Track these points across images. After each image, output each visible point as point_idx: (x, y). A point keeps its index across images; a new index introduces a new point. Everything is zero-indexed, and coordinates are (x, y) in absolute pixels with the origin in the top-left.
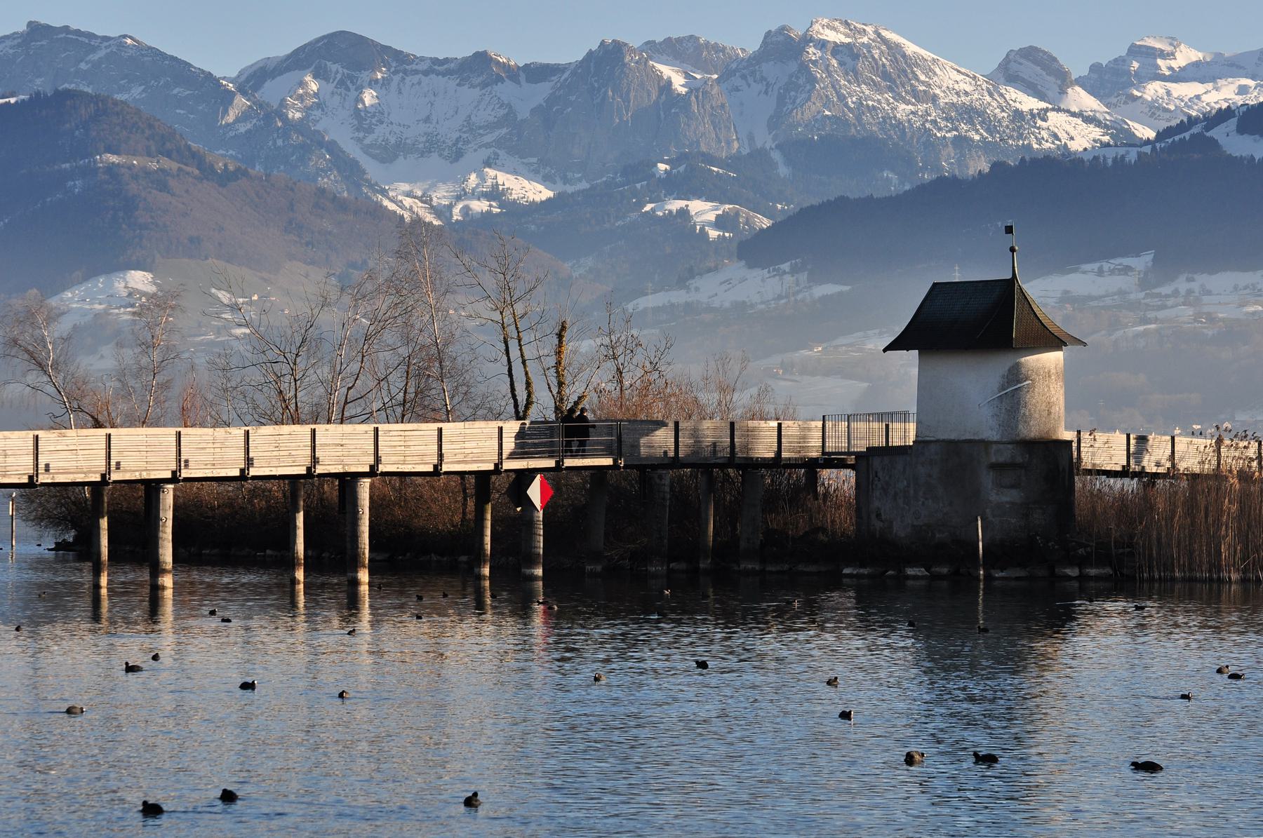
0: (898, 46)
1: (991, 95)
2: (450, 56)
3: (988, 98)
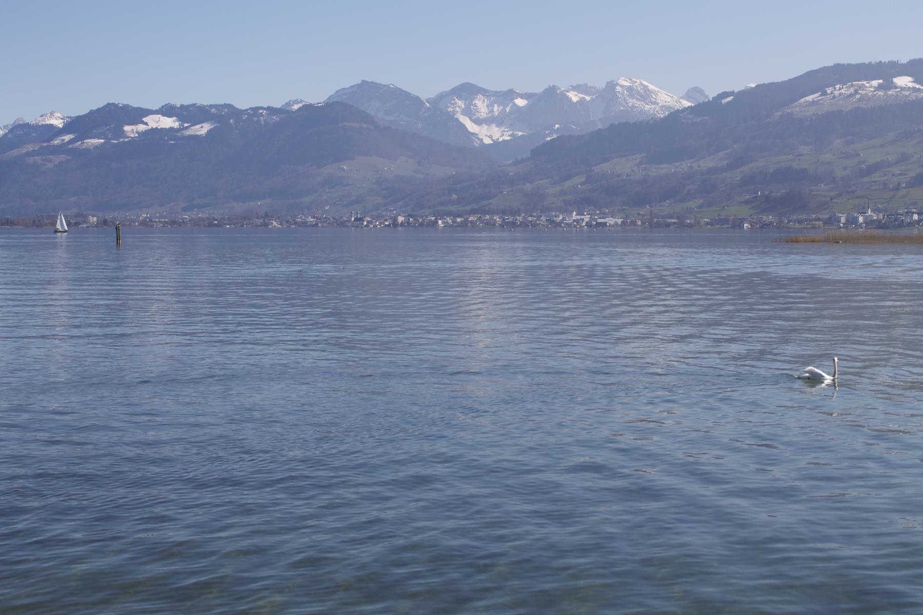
0: (647, 86)
1: (677, 102)
2: (501, 90)
3: (676, 103)
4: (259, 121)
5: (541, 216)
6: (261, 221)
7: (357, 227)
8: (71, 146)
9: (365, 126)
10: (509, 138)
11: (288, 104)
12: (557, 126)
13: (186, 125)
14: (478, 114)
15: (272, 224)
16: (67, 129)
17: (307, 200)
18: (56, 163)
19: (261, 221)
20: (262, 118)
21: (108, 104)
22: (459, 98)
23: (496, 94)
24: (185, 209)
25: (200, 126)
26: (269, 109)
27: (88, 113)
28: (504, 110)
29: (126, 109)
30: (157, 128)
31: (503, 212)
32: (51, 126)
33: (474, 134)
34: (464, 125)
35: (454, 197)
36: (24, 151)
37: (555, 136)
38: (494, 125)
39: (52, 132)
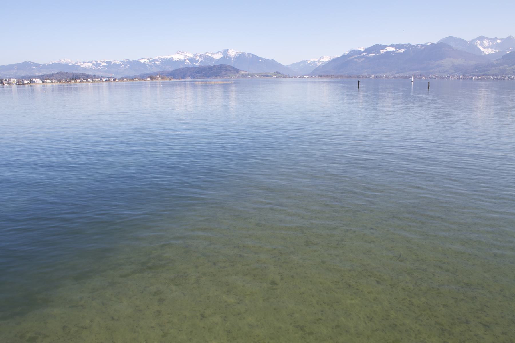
4: (418, 48)
5: (506, 77)
6: (419, 77)
7: (448, 79)
8: (366, 56)
9: (449, 49)
10: (494, 52)
11: (426, 43)
12: (511, 48)
13: (397, 50)
14: (484, 45)
15: (423, 78)
16: (365, 51)
17: (431, 71)
18: (362, 60)
19: (419, 77)
20: (419, 48)
21: (376, 44)
22: (479, 40)
23: (491, 39)
24: (396, 73)
25: (401, 50)
26: (421, 45)
27: (370, 47)
28: (493, 44)
29: (381, 45)
30: (389, 51)
31: (493, 75)
32: (360, 51)
33: (483, 51)
34: (480, 49)
35: (477, 70)
36: (353, 57)
37: (510, 52)
38: (489, 49)
39: (360, 52)
